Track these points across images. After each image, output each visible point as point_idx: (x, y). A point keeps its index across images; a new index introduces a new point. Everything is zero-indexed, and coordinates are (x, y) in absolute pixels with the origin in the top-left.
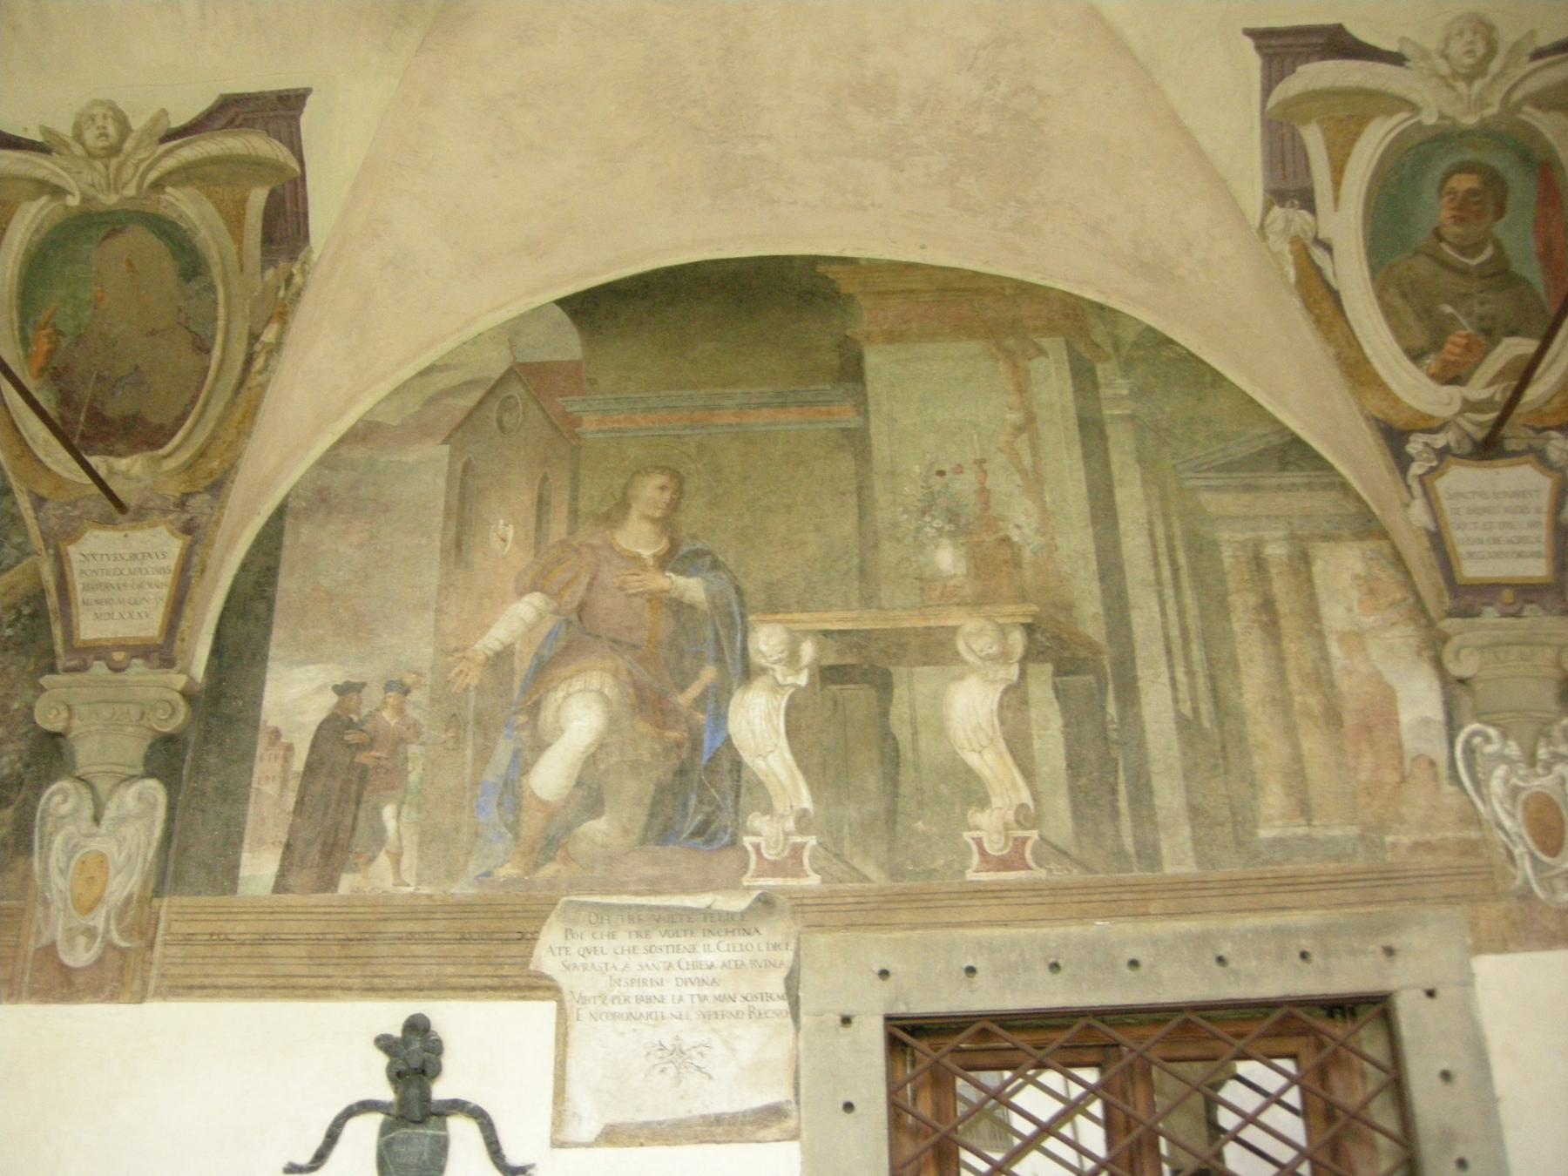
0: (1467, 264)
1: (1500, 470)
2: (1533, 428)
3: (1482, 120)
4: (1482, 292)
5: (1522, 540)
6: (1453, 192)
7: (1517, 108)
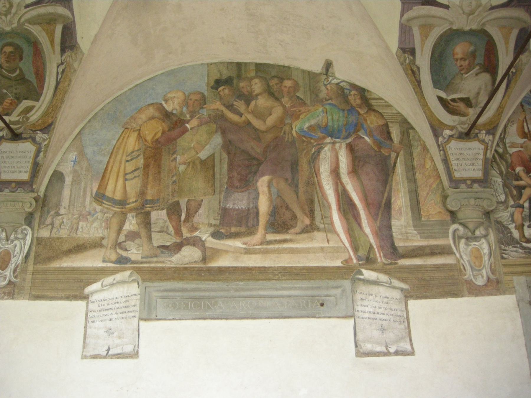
0: (10, 76)
1: (19, 144)
2: (32, 130)
3: (12, 28)
4: (16, 85)
5: (22, 167)
6: (5, 52)
7: (23, 24)
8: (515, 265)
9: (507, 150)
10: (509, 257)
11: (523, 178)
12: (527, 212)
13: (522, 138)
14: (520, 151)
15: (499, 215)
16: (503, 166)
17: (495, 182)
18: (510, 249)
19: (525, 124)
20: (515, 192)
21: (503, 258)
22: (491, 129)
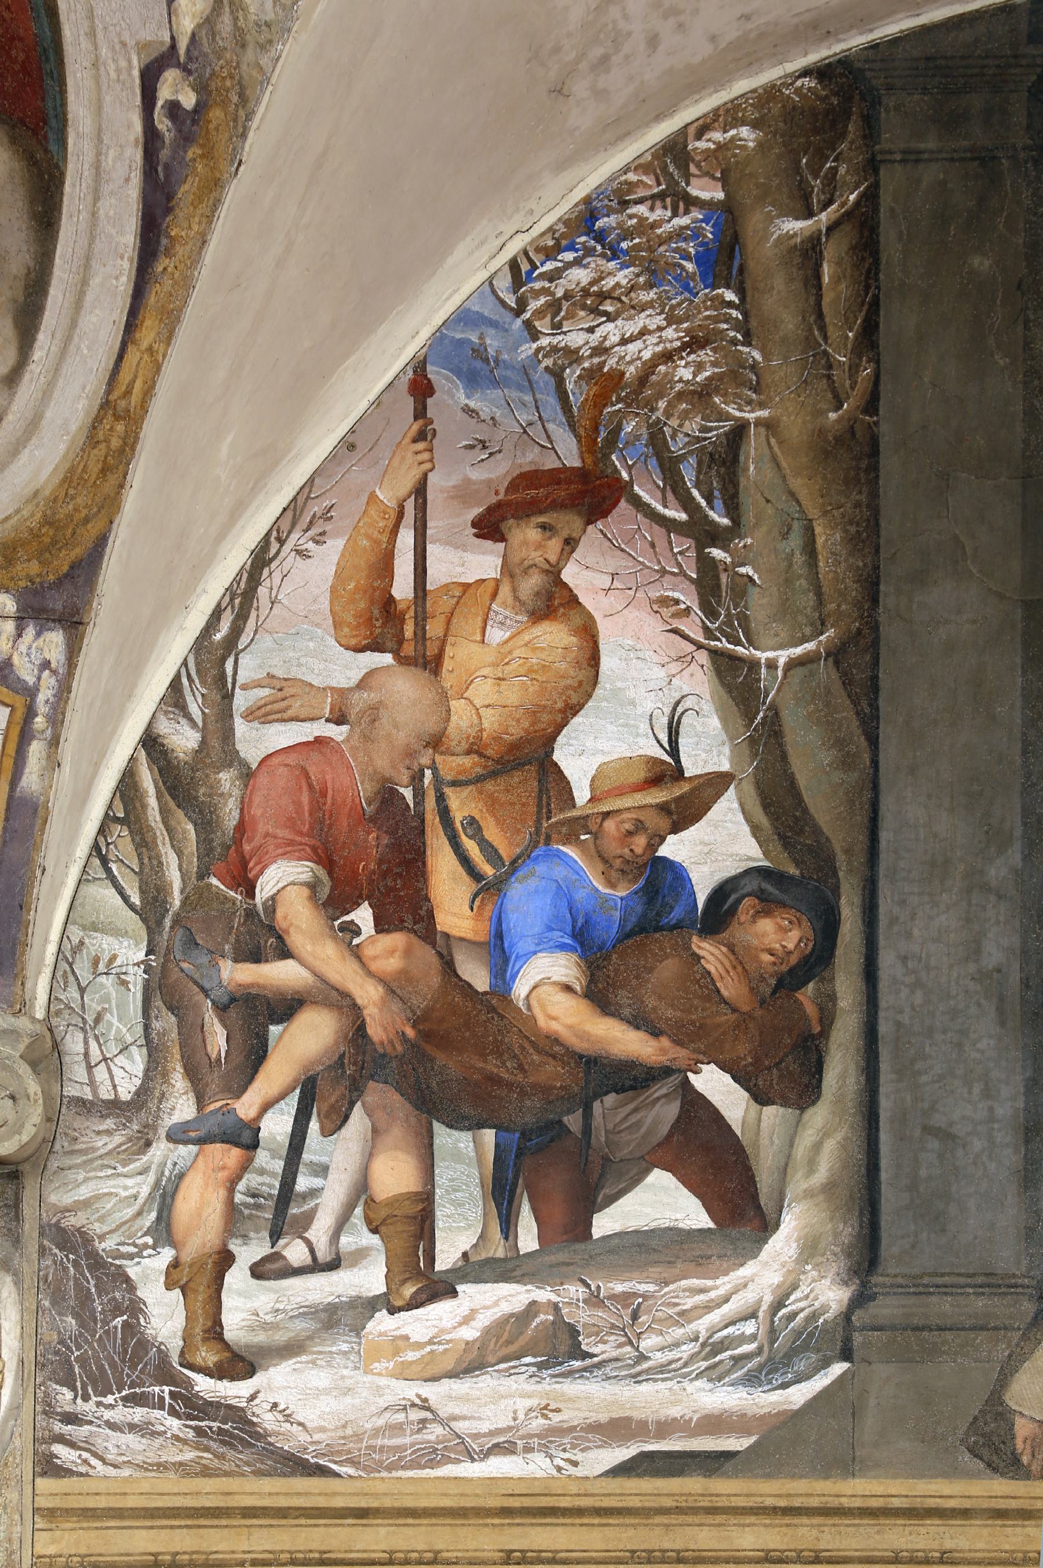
8: (118, 1513)
9: (228, 734)
10: (94, 1461)
11: (296, 940)
12: (273, 1175)
13: (359, 649)
14: (320, 742)
15: (84, 1192)
16: (179, 854)
17: (102, 968)
18: (108, 1415)
19: (406, 538)
20: (218, 1039)
21: (48, 1467)
22: (59, 583)
